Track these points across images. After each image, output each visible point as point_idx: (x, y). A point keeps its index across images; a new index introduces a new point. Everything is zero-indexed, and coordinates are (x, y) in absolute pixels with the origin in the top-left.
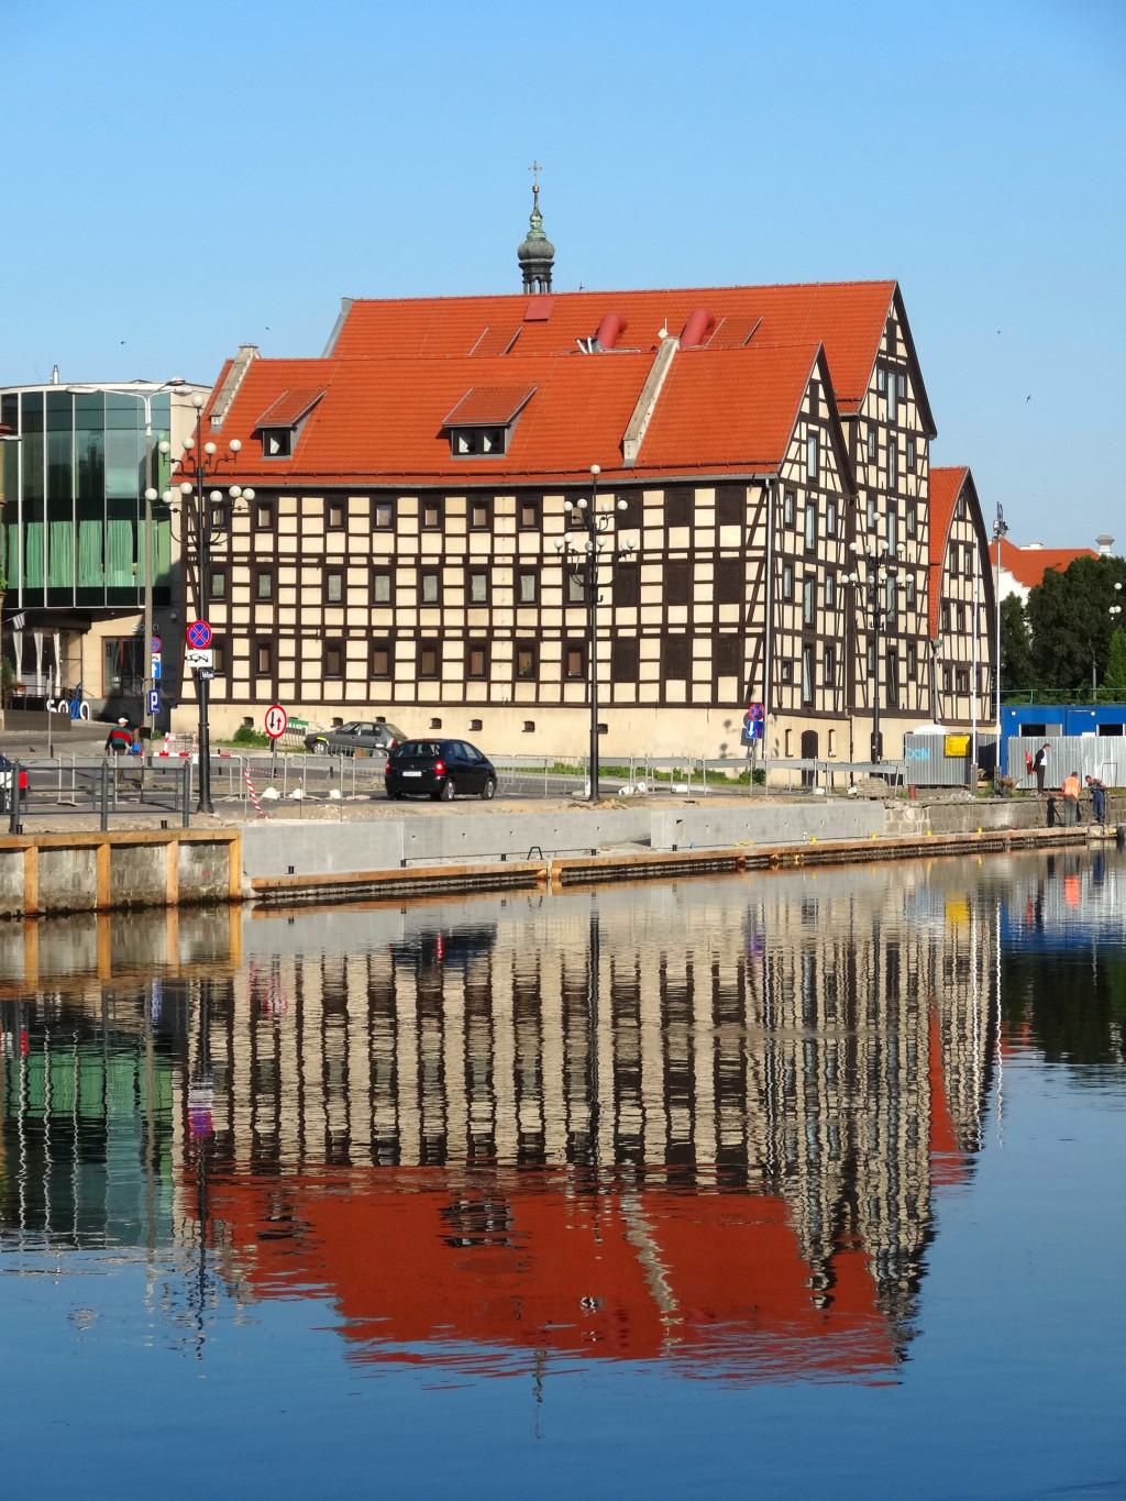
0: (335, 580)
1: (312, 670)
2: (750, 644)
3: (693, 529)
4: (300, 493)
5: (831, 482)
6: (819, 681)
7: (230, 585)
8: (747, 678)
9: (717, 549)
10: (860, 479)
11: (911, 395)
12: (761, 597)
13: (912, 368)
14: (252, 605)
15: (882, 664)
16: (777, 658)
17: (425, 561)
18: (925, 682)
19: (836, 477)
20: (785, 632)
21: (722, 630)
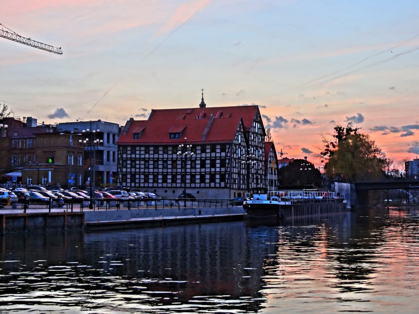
0: (147, 163)
1: (142, 181)
2: (227, 176)
3: (216, 153)
4: (140, 146)
5: (244, 144)
6: (241, 183)
7: (127, 164)
8: (226, 182)
9: (220, 157)
10: (250, 143)
11: (261, 127)
12: (229, 166)
14: (131, 168)
15: (255, 180)
16: (232, 178)
17: (164, 159)
18: (264, 183)
19: (245, 143)
20: (234, 173)
21: (222, 173)
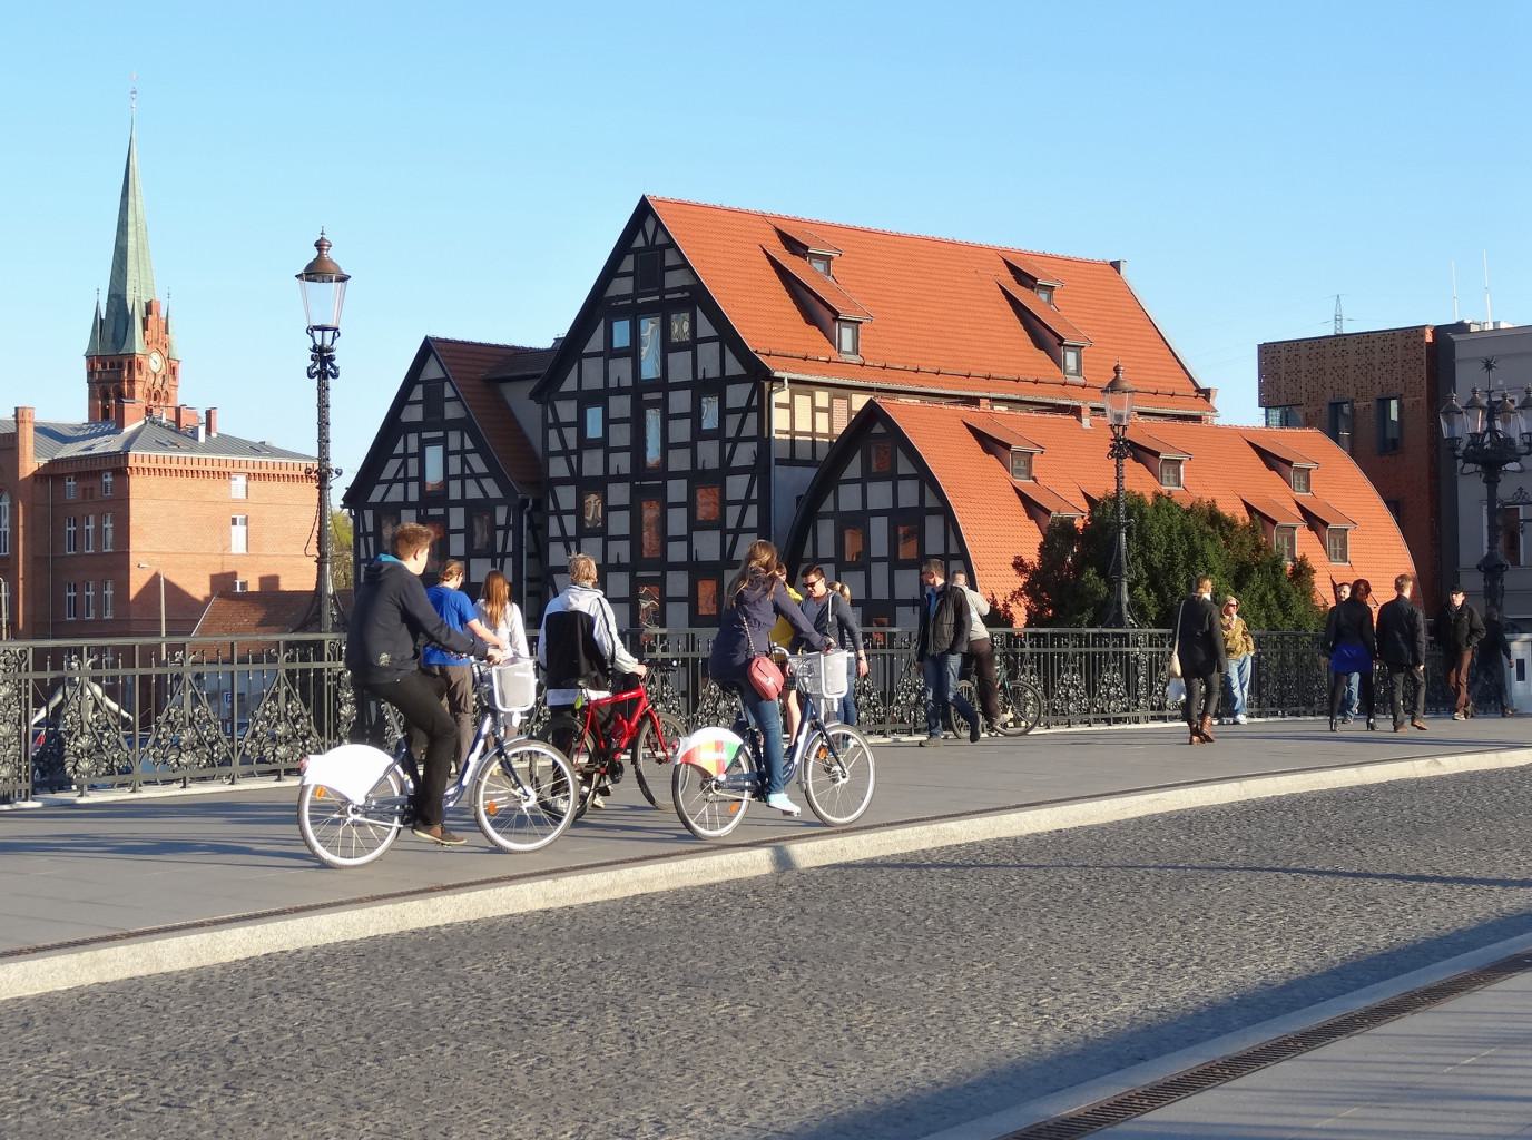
11: (706, 328)
13: (698, 298)
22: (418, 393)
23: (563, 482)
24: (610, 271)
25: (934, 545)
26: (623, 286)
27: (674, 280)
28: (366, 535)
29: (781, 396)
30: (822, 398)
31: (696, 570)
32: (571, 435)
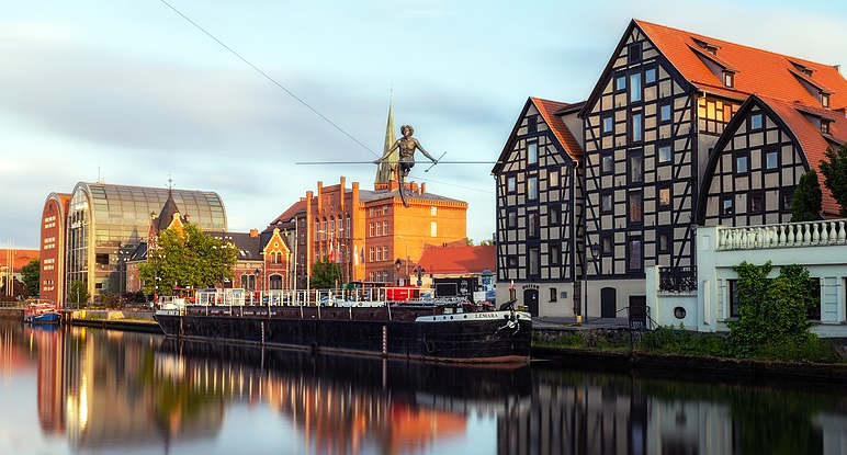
11: (663, 74)
13: (661, 61)
22: (525, 122)
23: (593, 153)
24: (616, 56)
25: (787, 158)
26: (621, 62)
27: (646, 55)
28: (502, 186)
29: (701, 102)
30: (719, 105)
31: (660, 185)
32: (597, 132)
